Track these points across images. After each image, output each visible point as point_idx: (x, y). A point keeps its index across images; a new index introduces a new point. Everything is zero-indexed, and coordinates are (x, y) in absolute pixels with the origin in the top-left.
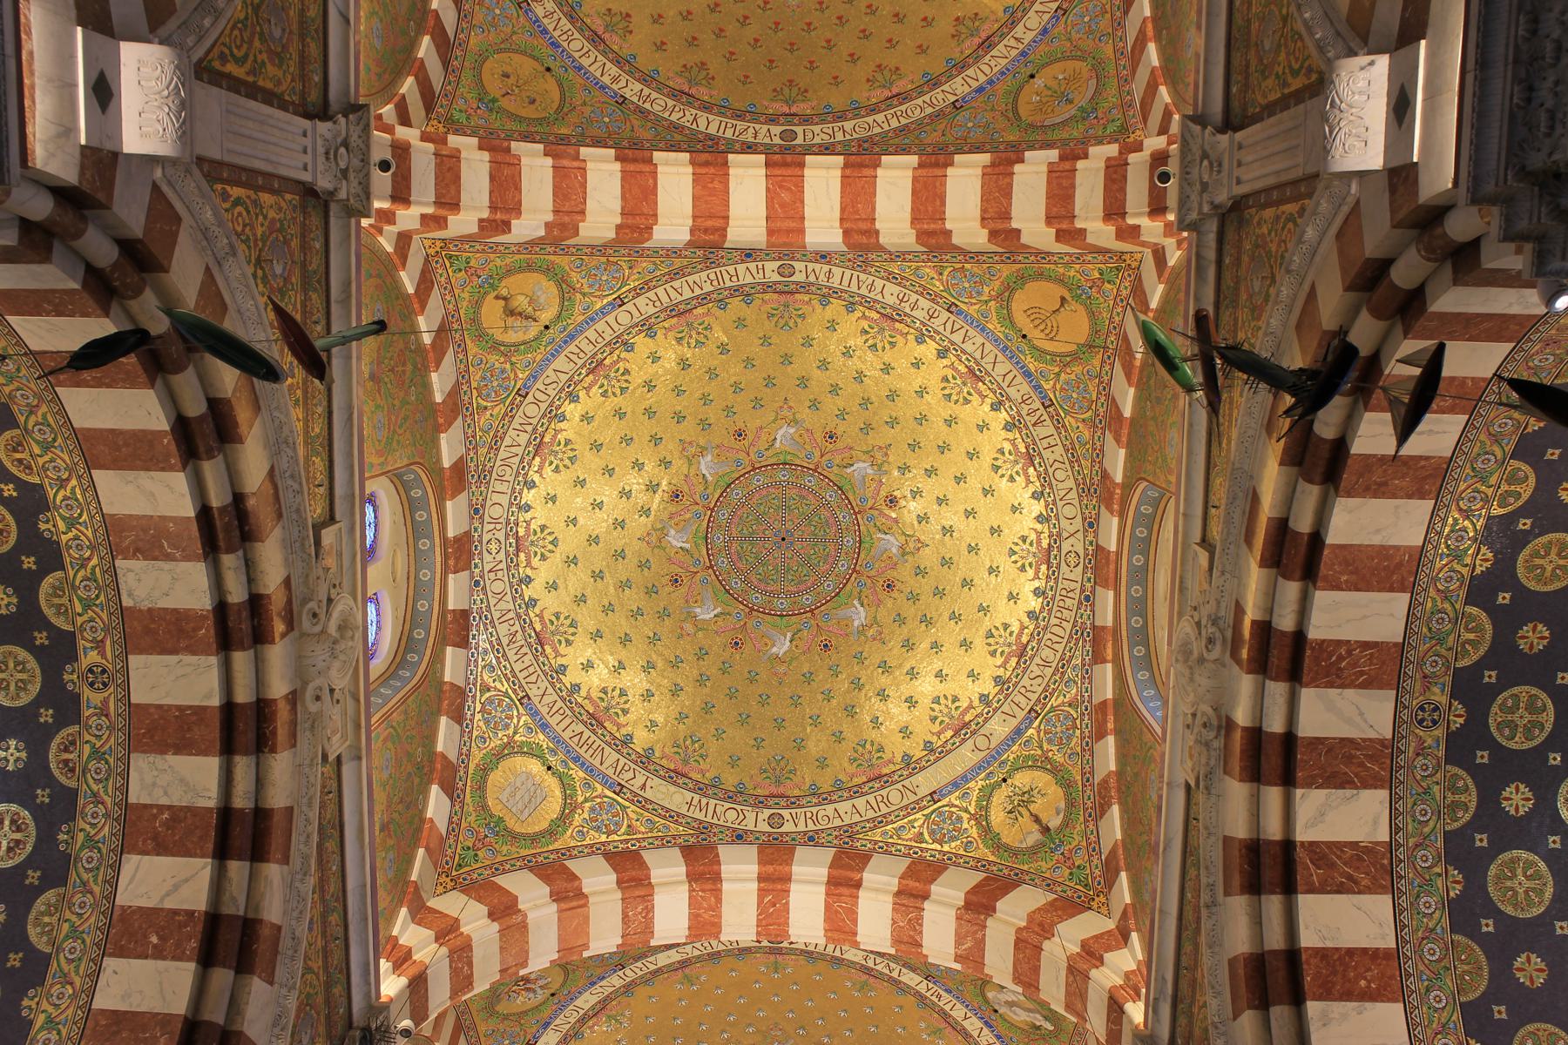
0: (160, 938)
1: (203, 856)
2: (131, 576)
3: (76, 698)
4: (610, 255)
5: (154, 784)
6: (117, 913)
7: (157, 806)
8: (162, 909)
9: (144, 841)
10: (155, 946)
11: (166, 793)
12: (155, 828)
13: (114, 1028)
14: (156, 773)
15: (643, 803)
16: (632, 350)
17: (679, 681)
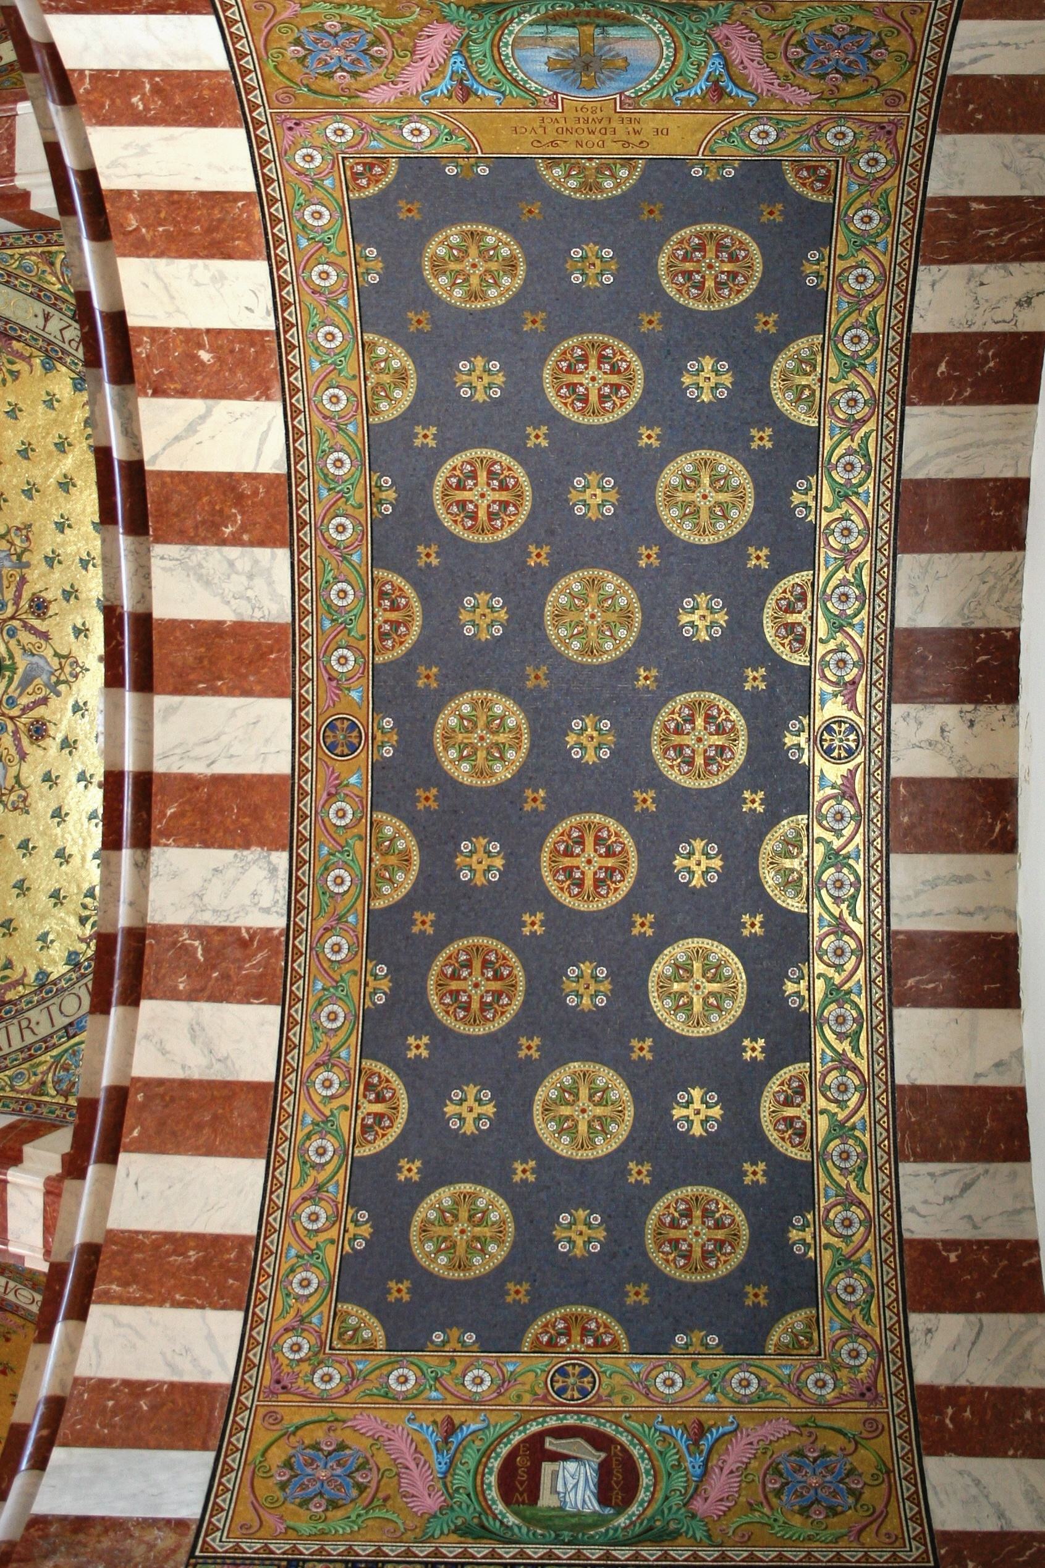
0: (196, 358)
1: (160, 474)
2: (266, 902)
3: (380, 704)
4: (62, 1106)
5: (251, 577)
6: (276, 389)
7: (242, 544)
8: (205, 396)
9: (256, 493)
10: (201, 346)
11: (231, 564)
12: (243, 513)
13: (218, 236)
14: (250, 593)
15: (39, 294)
16: (70, 954)
17: (25, 463)
